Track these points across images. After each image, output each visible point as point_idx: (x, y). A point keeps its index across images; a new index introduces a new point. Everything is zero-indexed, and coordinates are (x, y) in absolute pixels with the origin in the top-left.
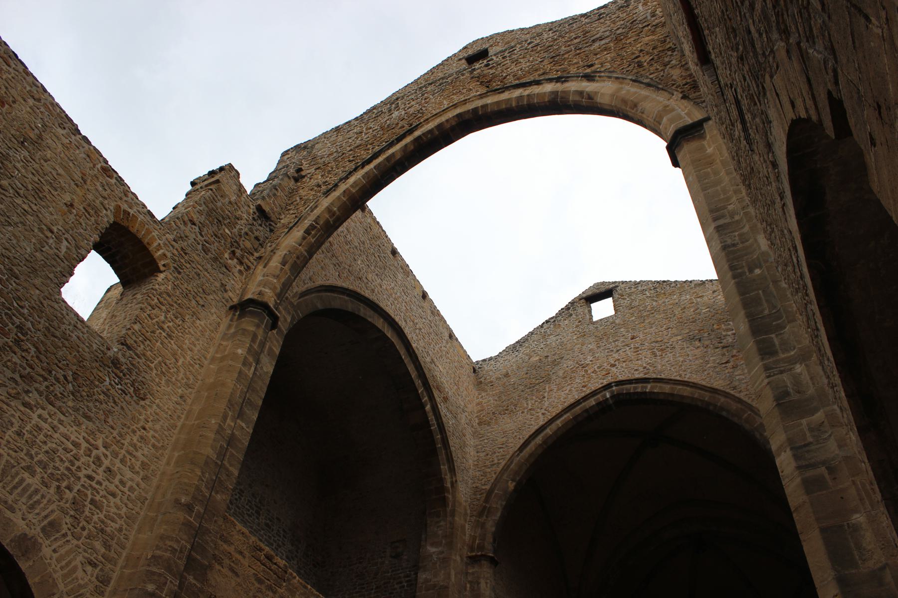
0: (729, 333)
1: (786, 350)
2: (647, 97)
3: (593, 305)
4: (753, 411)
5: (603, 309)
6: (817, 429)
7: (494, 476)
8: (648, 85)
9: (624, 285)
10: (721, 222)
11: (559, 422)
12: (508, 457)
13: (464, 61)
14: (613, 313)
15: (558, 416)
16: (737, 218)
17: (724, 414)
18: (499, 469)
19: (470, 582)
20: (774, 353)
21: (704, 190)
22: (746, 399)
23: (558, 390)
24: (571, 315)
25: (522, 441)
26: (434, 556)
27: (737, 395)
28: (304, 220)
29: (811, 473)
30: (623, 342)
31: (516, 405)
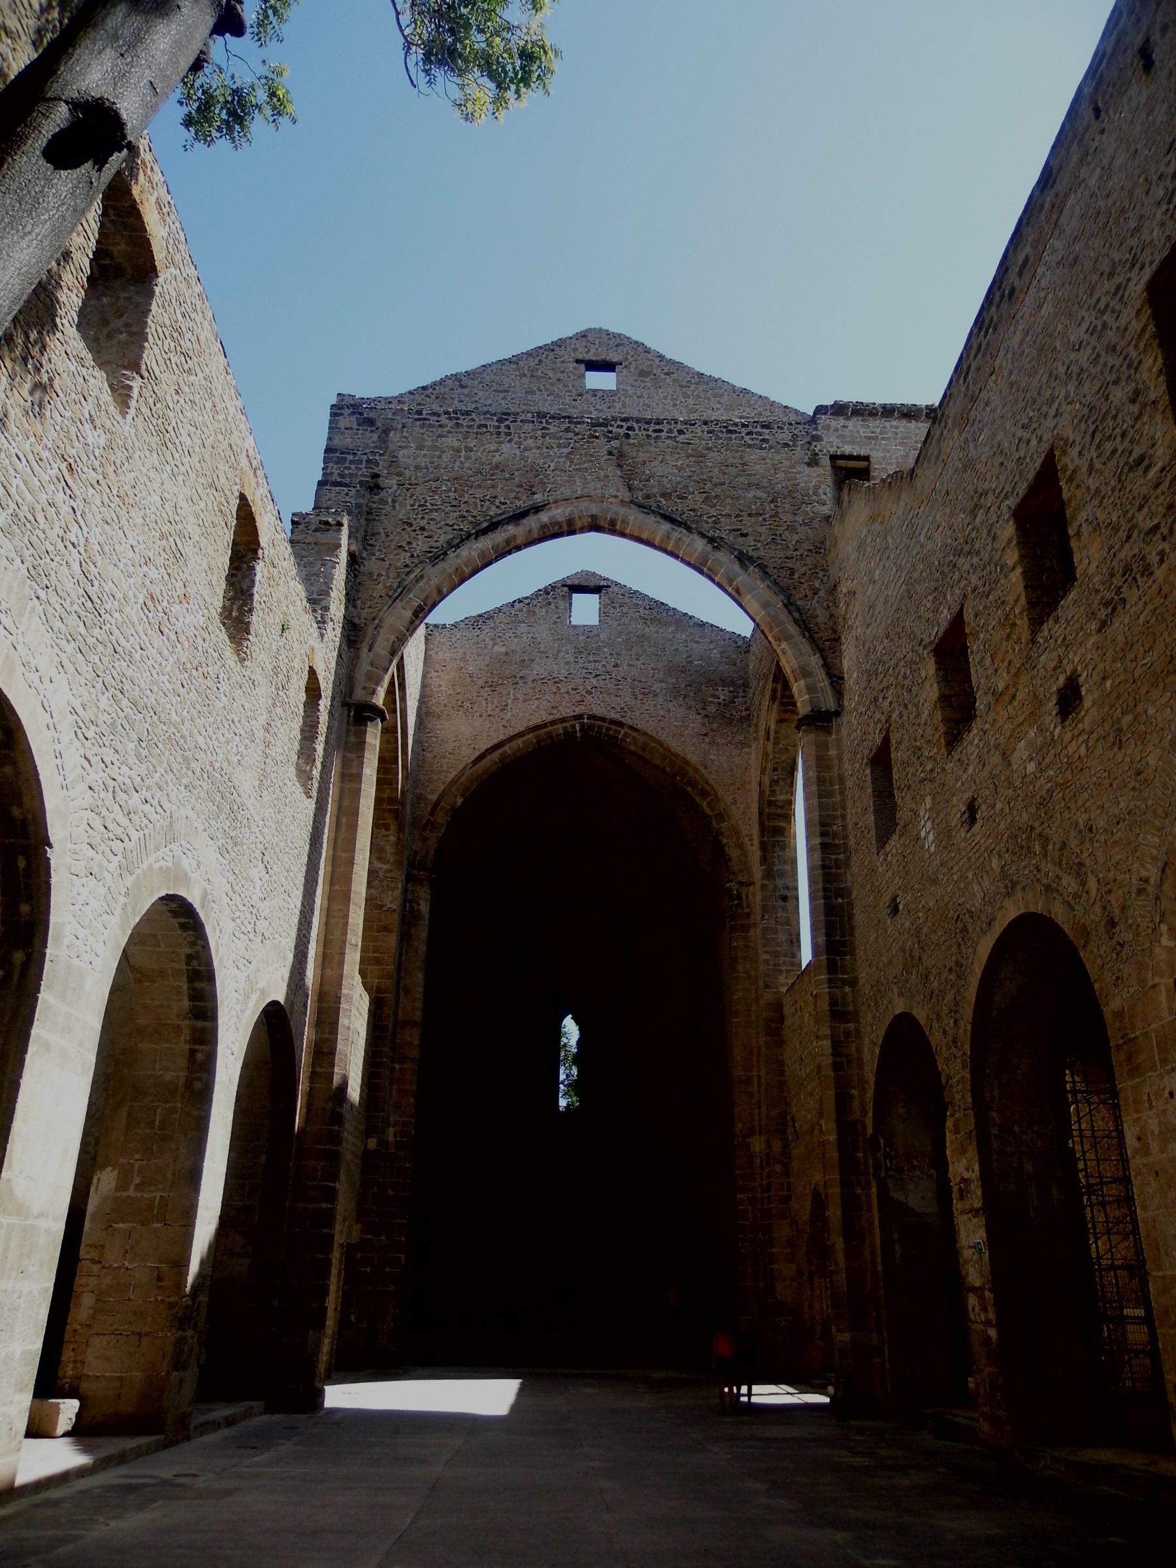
0: (716, 701)
1: (843, 973)
4: (716, 796)
5: (585, 610)
6: (847, 1033)
7: (443, 787)
8: (796, 622)
9: (616, 589)
11: (520, 741)
12: (460, 767)
13: (583, 366)
15: (520, 735)
16: (837, 842)
17: (689, 789)
18: (449, 780)
19: (411, 901)
20: (836, 972)
21: (820, 797)
22: (712, 783)
23: (524, 701)
24: (550, 603)
25: (477, 754)
26: (381, 874)
27: (707, 776)
28: (410, 591)
29: (838, 1059)
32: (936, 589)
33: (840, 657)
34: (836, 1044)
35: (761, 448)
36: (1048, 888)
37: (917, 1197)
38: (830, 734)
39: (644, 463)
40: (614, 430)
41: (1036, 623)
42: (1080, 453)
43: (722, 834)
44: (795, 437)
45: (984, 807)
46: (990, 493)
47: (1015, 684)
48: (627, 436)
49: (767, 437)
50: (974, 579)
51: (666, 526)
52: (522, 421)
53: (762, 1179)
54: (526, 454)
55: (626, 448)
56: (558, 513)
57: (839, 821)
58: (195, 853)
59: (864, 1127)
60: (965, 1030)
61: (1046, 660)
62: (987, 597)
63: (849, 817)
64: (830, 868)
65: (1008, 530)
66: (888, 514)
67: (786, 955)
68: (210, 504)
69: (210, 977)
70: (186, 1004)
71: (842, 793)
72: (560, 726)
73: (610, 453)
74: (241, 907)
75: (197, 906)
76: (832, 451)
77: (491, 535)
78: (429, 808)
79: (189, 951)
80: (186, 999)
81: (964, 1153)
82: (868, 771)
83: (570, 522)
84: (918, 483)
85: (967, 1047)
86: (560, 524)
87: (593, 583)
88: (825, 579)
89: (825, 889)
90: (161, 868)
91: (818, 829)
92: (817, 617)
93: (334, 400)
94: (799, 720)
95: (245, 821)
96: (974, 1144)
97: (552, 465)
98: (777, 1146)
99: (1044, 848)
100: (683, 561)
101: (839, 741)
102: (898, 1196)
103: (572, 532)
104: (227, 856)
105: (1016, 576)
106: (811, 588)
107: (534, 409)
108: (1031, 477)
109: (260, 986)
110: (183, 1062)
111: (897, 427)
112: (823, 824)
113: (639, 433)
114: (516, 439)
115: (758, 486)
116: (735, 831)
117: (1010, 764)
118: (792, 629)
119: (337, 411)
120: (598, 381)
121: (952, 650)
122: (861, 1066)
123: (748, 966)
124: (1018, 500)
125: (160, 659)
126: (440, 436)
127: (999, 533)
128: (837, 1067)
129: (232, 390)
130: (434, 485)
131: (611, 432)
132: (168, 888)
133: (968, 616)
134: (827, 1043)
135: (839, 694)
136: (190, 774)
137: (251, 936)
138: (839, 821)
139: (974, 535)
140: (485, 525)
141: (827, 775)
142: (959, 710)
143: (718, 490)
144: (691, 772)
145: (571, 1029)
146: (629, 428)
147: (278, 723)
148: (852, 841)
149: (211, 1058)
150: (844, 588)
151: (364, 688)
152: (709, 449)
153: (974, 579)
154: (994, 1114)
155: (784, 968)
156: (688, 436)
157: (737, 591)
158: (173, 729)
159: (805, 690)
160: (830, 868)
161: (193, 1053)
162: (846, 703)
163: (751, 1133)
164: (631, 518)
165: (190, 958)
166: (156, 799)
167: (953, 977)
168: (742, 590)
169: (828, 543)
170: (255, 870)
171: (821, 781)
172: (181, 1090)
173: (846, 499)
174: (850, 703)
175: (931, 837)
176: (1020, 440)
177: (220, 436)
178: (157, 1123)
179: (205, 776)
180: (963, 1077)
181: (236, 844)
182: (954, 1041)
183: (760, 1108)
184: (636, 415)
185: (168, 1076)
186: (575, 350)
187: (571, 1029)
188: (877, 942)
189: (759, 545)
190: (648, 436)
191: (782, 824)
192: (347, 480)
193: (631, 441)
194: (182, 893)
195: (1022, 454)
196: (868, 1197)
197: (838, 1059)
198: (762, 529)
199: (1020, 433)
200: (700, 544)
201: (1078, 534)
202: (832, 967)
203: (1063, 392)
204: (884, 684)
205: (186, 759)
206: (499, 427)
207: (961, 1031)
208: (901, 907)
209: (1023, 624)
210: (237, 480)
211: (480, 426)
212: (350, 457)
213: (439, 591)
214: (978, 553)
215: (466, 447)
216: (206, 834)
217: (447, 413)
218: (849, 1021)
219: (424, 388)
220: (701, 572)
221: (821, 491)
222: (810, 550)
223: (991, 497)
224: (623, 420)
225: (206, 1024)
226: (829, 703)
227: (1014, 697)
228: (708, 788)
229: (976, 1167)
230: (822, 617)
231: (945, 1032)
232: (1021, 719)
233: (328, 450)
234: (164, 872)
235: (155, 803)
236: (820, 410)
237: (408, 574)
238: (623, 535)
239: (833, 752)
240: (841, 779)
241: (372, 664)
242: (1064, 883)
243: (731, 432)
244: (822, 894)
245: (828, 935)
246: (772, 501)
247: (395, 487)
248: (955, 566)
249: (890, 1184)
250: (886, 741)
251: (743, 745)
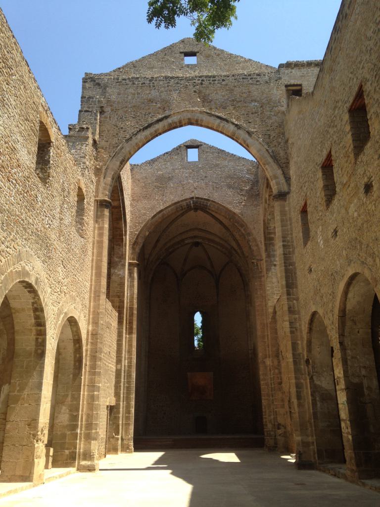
1: (293, 295)
2: (270, 163)
3: (188, 150)
4: (247, 226)
5: (193, 155)
6: (295, 319)
7: (140, 229)
10: (285, 243)
11: (169, 209)
13: (183, 54)
14: (197, 160)
16: (289, 244)
17: (236, 224)
20: (290, 295)
21: (282, 227)
27: (243, 218)
29: (292, 329)
30: (201, 177)
31: (150, 196)
32: (322, 142)
33: (289, 169)
34: (291, 323)
35: (257, 85)
36: (363, 262)
37: (324, 383)
38: (286, 201)
39: (209, 95)
40: (196, 81)
41: (357, 155)
42: (371, 84)
43: (250, 241)
44: (270, 79)
45: (339, 230)
46: (340, 102)
47: (349, 181)
48: (202, 84)
49: (259, 79)
50: (335, 137)
51: (218, 121)
52: (159, 80)
53: (270, 375)
54: (161, 94)
55: (202, 89)
56: (175, 118)
57: (290, 236)
58: (32, 264)
59: (303, 355)
60: (336, 319)
61: (360, 171)
62: (339, 144)
63: (294, 234)
64: (286, 254)
65: (346, 117)
66: (305, 110)
67: (276, 287)
68: (26, 127)
69: (42, 310)
70: (33, 321)
71: (291, 224)
72: (185, 202)
73: (195, 92)
74: (53, 282)
75: (33, 284)
76: (286, 83)
77: (149, 129)
78: (136, 236)
79: (33, 301)
80: (33, 319)
81: (338, 367)
82: (300, 216)
83: (180, 122)
84: (315, 97)
85: (337, 325)
86: (176, 123)
87: (195, 145)
88: (283, 138)
89: (285, 263)
90: (16, 271)
91: (281, 239)
92: (280, 154)
93: (84, 76)
94: (274, 196)
95: (53, 250)
96: (341, 363)
97: (172, 98)
98: (276, 363)
99: (361, 247)
100: (226, 135)
101: (289, 204)
102: (318, 383)
103: (181, 126)
104: (46, 264)
105: (349, 136)
106: (277, 142)
107: (163, 75)
108: (354, 94)
109: (64, 312)
110: (33, 343)
111: (313, 71)
112: (283, 237)
113: (206, 83)
114: (157, 88)
115: (255, 101)
116: (255, 240)
117: (348, 213)
118: (270, 160)
119: (85, 81)
120: (191, 60)
121: (327, 167)
122: (301, 332)
123: (261, 292)
124: (350, 104)
125: (9, 191)
126: (126, 89)
127: (343, 118)
128: (292, 332)
129: (32, 79)
130: (126, 109)
131: (195, 83)
132: (20, 278)
133: (333, 153)
134: (288, 323)
135: (289, 185)
136: (27, 234)
137: (59, 293)
138: (290, 236)
139: (335, 119)
140: (146, 125)
141: (284, 218)
142: (330, 192)
143: (239, 104)
144: (237, 217)
145: (198, 318)
146: (203, 80)
147: (66, 210)
148: (295, 244)
149: (44, 341)
150: (290, 142)
151: (103, 193)
152: (235, 87)
153: (335, 137)
154: (349, 351)
155: (276, 292)
156: (227, 82)
157: (248, 146)
158: (17, 218)
159: (275, 184)
160: (286, 254)
161: (37, 339)
162: (291, 188)
163: (266, 357)
164: (204, 118)
165: (33, 303)
166: (12, 245)
167: (331, 297)
168: (249, 145)
169: (284, 123)
170: (60, 268)
171: (282, 221)
172: (33, 354)
173: (290, 104)
174: (294, 187)
175: (322, 242)
176: (350, 78)
177: (29, 99)
178: (24, 366)
179: (34, 234)
180: (336, 337)
181: (50, 259)
182: (333, 323)
183: (268, 347)
184: (205, 74)
185: (28, 348)
186: (180, 48)
187: (198, 318)
188: (306, 284)
189: (256, 126)
190: (210, 83)
191: (272, 236)
192: (90, 110)
193: (203, 86)
194: (27, 280)
195: (351, 84)
196: (306, 383)
197: (292, 329)
198: (257, 119)
199: (350, 75)
200: (232, 128)
201: (371, 118)
202: (288, 294)
203: (365, 58)
204: (304, 181)
205: (24, 229)
206: (150, 84)
207: (335, 319)
208: (312, 270)
209: (352, 156)
210: (38, 116)
211: (142, 84)
212: (91, 100)
213: (130, 153)
214: (336, 126)
215: (137, 92)
216: (36, 256)
217: (129, 79)
218: (296, 315)
219: (119, 69)
220: (233, 139)
221: (281, 101)
222: (277, 126)
223: (340, 103)
224: (200, 77)
225: (42, 328)
226: (285, 188)
227: (349, 186)
228: (244, 224)
229: (342, 372)
230: (282, 153)
231: (329, 319)
232: (352, 195)
233: (82, 97)
234: (18, 273)
235: (12, 247)
236: (281, 66)
237: (117, 147)
238: (201, 126)
239: (287, 209)
240: (290, 219)
241: (105, 184)
242: (368, 260)
243: (243, 78)
244: (283, 265)
245: (287, 281)
246: (261, 107)
247: (110, 111)
248: (328, 132)
249: (315, 378)
250: (306, 204)
251: (257, 205)
